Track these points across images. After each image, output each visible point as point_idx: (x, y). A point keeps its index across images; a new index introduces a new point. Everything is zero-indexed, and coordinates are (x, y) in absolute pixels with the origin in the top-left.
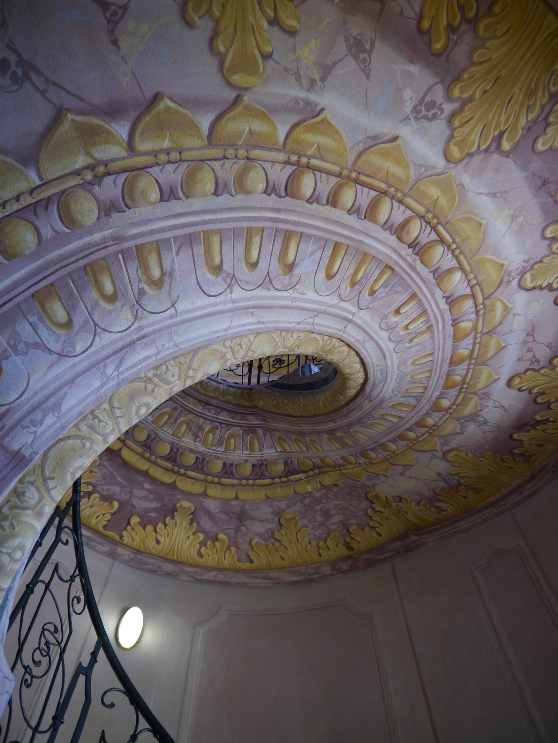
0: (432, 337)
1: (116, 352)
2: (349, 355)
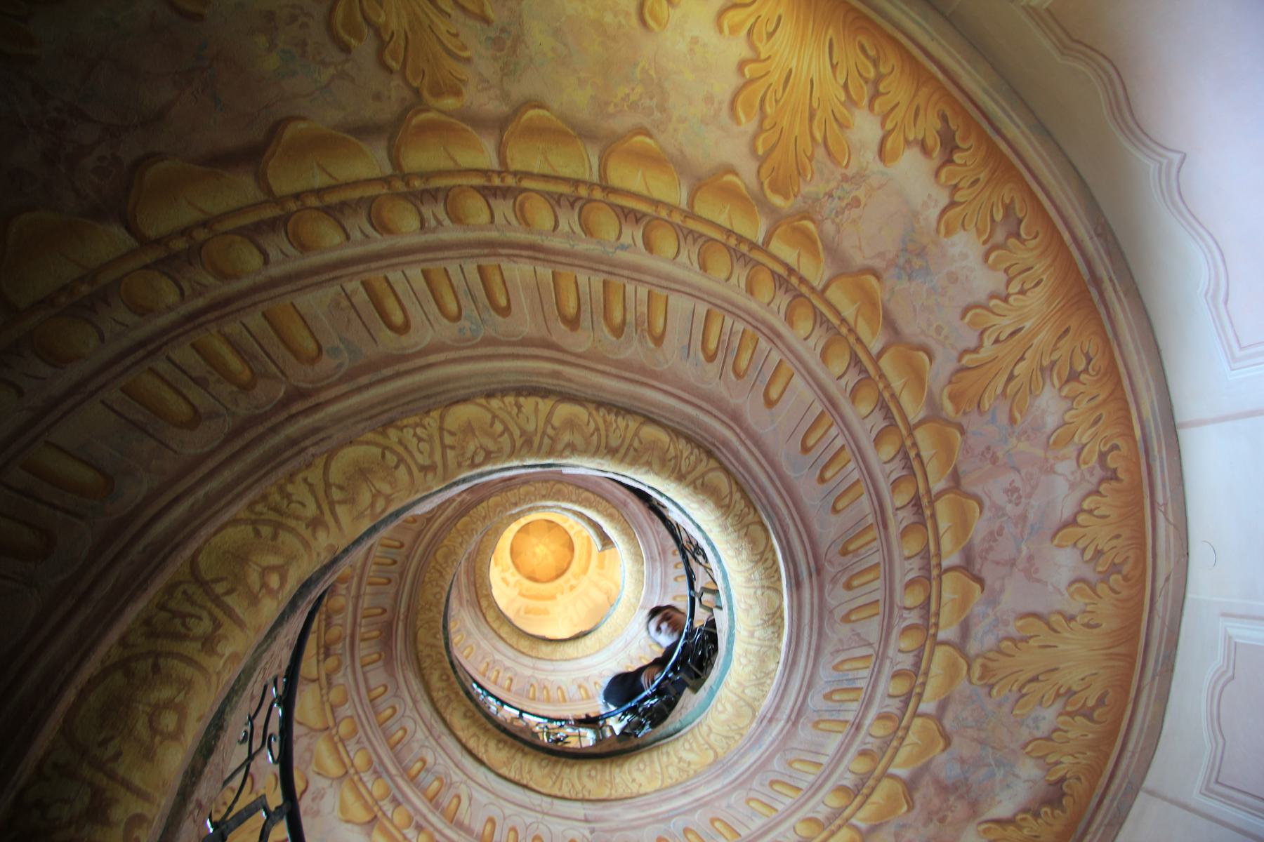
0: (477, 669)
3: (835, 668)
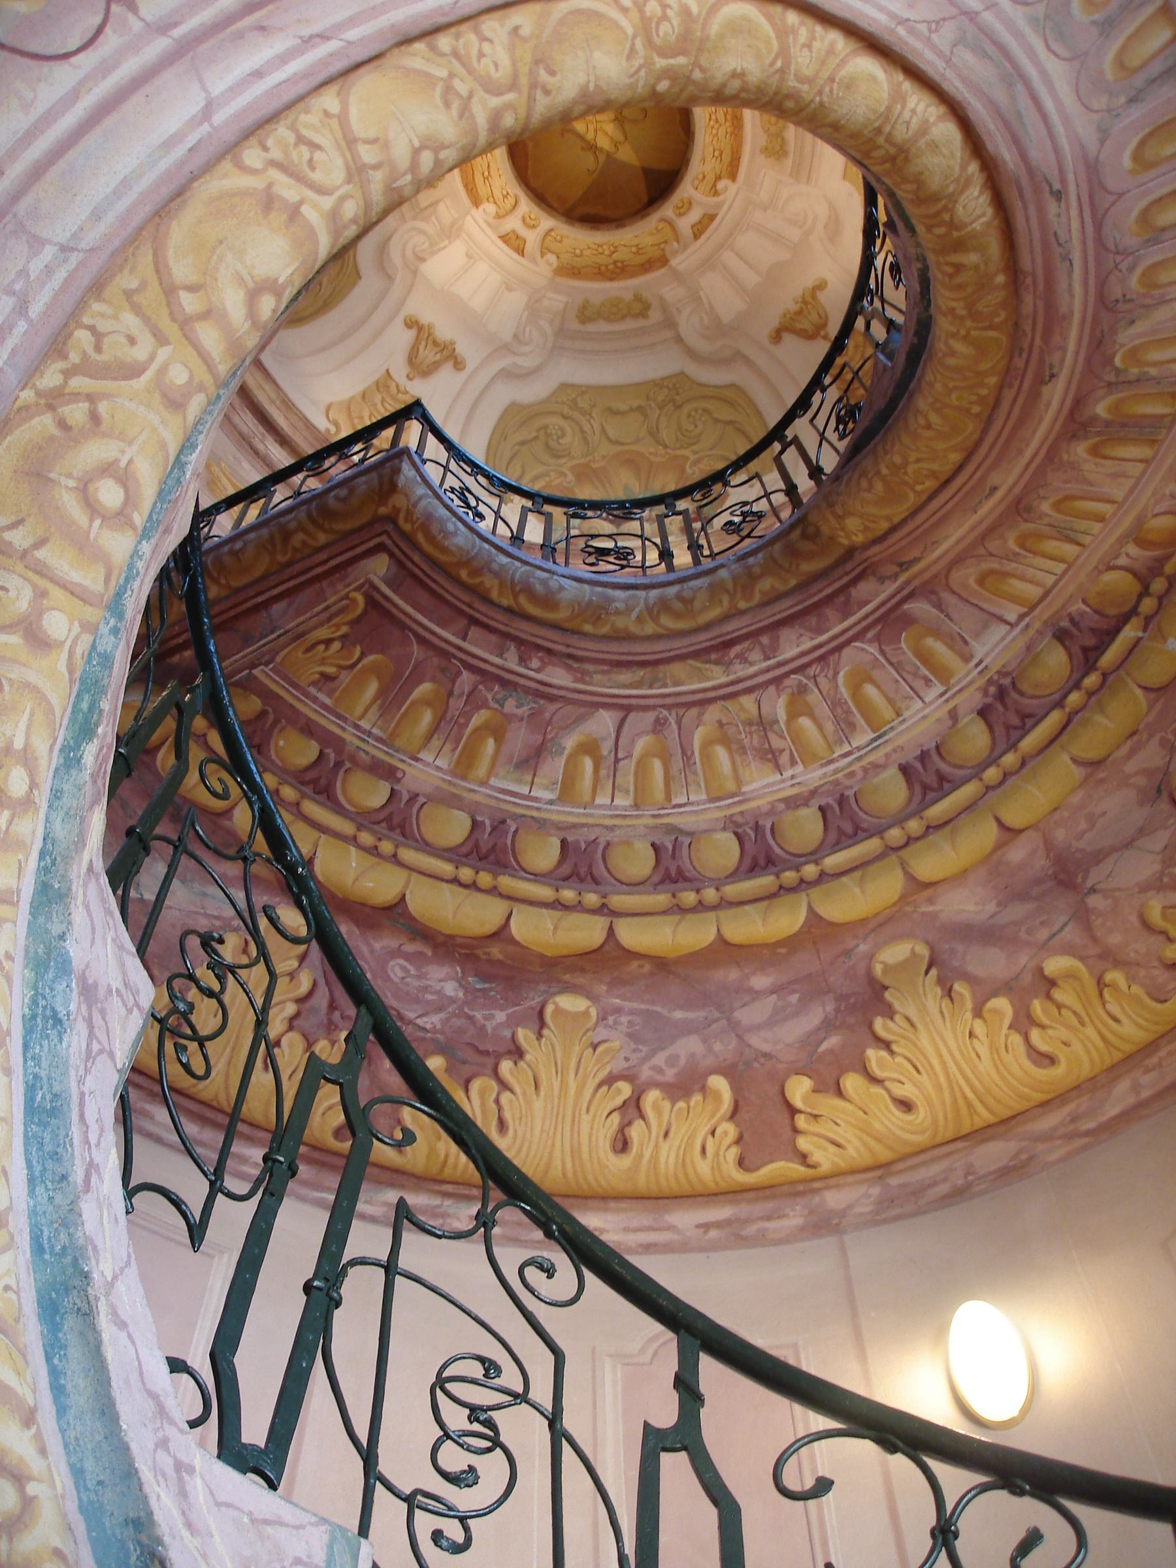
2: (783, 33)
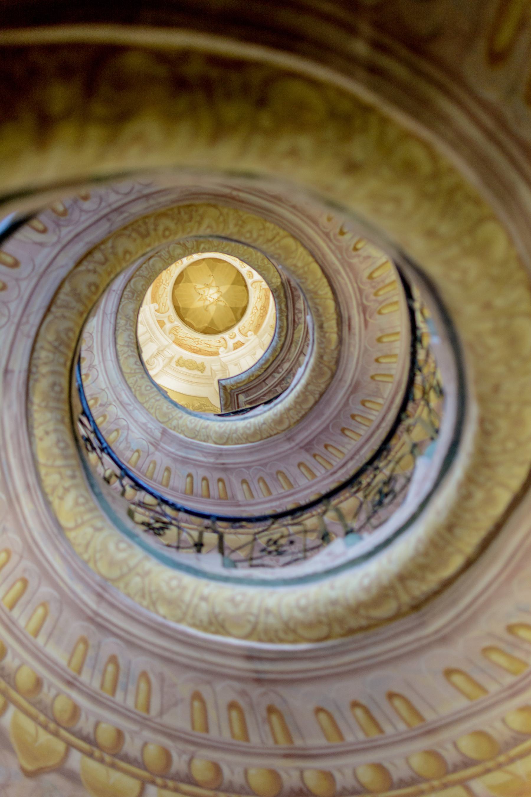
1: (124, 408)
3: (144, 675)
